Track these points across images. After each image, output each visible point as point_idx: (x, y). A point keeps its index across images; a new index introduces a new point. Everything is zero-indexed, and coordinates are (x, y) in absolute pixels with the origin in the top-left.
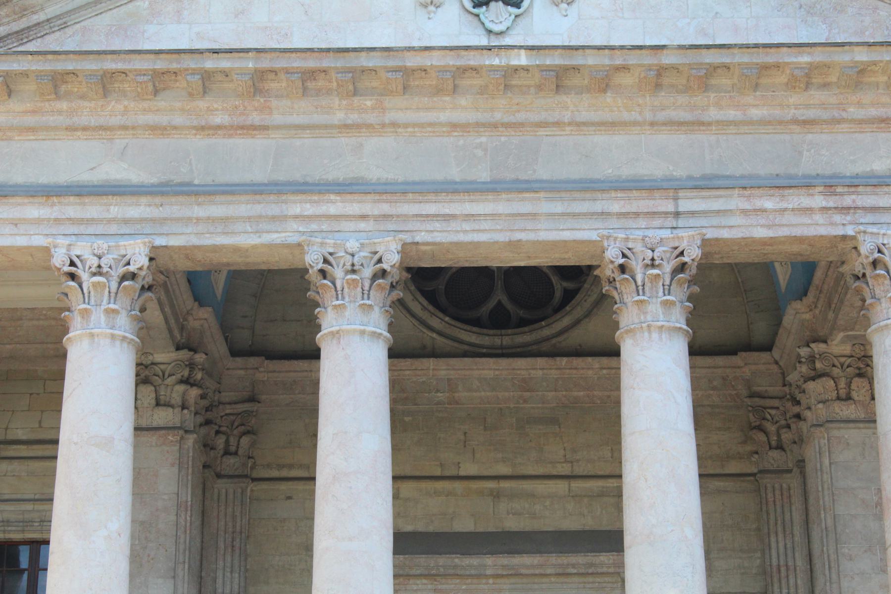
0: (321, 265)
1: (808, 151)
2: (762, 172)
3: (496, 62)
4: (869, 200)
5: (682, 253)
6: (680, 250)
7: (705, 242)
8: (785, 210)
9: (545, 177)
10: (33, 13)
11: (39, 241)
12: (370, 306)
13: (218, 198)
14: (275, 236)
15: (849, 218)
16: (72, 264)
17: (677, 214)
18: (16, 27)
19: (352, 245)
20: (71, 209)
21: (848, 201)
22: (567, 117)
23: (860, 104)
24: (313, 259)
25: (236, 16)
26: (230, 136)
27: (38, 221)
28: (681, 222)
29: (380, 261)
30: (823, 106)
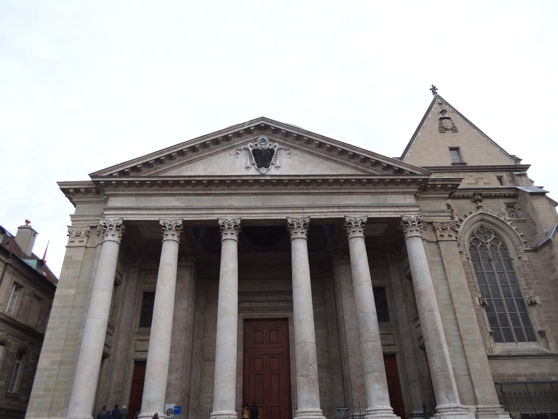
0: (222, 224)
1: (333, 199)
2: (323, 204)
3: (263, 178)
4: (347, 210)
5: (305, 221)
6: (305, 221)
7: (311, 219)
8: (328, 212)
9: (274, 205)
10: (159, 169)
11: (157, 219)
12: (233, 233)
13: (198, 210)
14: (212, 218)
15: (343, 214)
16: (164, 224)
17: (304, 213)
18: (154, 172)
19: (229, 219)
20: (165, 212)
21: (342, 210)
22: (279, 192)
23: (345, 189)
24: (220, 222)
25: (204, 170)
26: (202, 196)
27: (157, 214)
28: (305, 215)
29: (236, 223)
30: (336, 189)
